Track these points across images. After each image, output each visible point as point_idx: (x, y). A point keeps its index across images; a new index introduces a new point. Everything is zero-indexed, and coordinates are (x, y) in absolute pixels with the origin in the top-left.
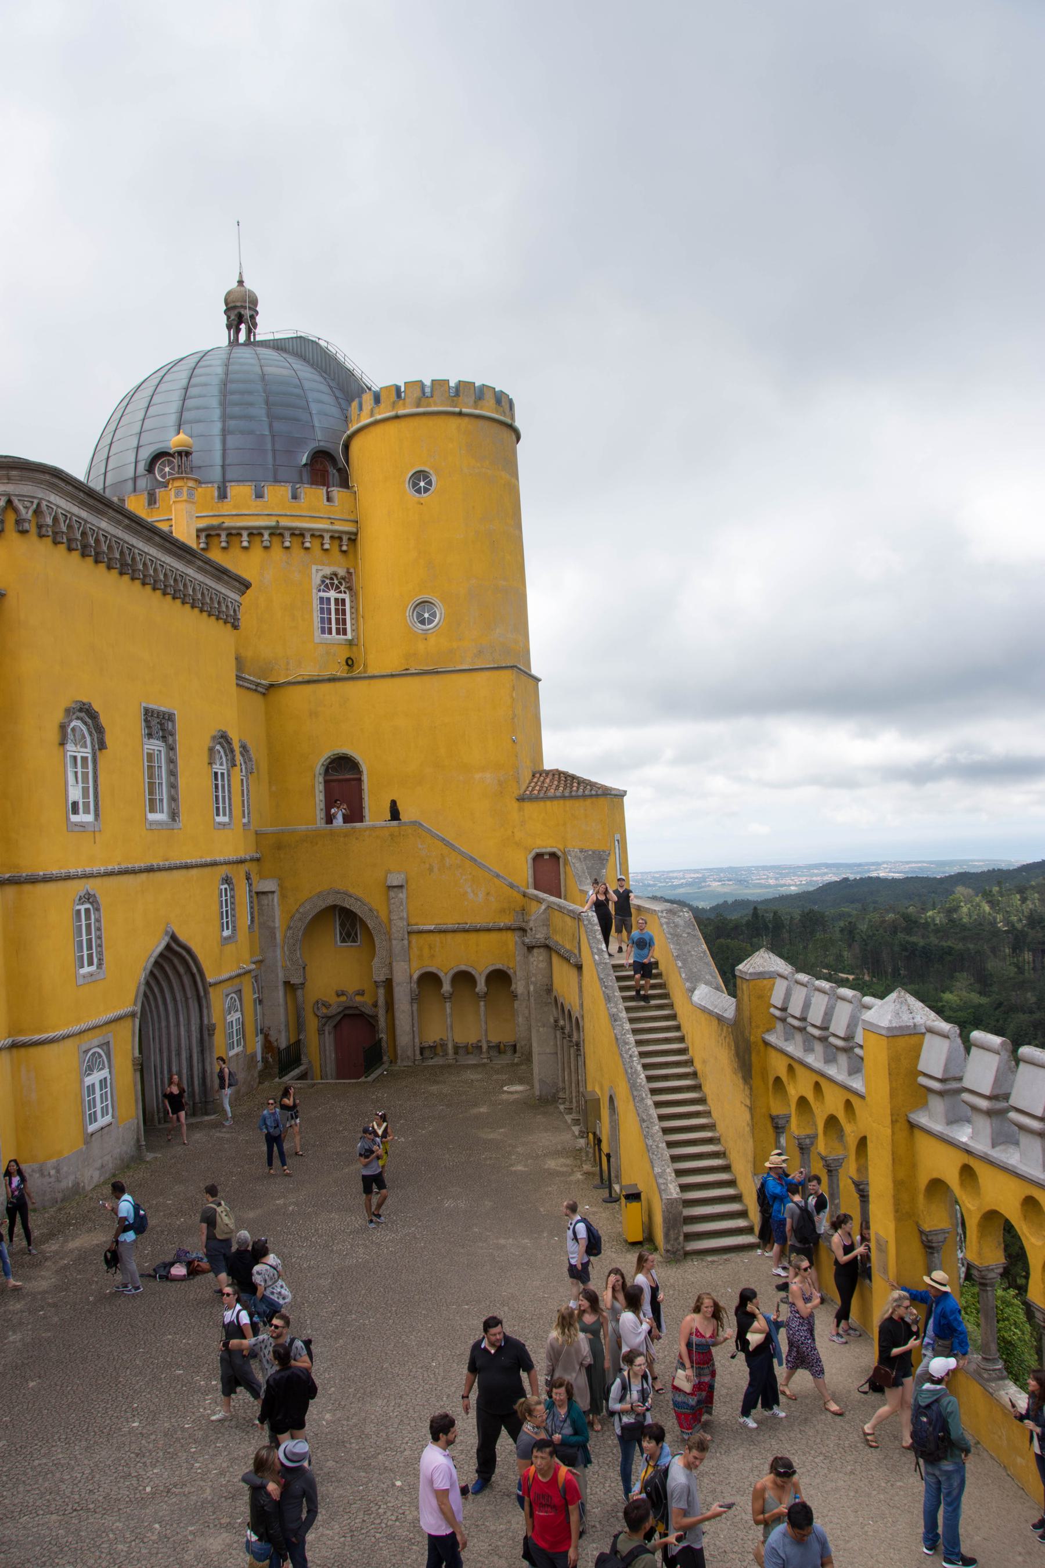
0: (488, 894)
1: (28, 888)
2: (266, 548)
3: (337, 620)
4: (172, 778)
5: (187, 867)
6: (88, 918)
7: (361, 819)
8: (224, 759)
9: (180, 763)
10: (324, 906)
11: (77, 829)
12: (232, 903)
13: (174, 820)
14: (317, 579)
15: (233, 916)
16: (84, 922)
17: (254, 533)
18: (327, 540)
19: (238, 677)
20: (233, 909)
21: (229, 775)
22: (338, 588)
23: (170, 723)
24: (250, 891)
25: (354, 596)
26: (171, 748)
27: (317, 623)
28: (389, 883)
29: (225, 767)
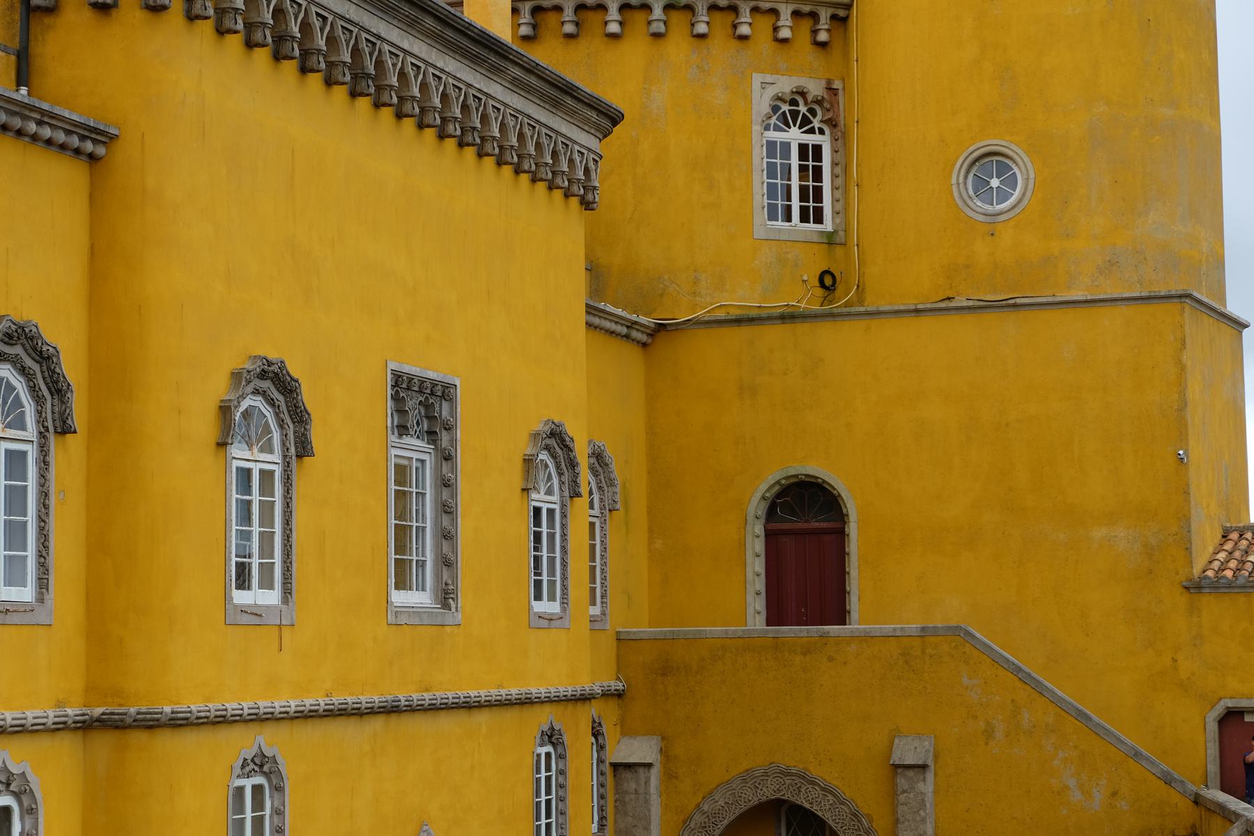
0: (1114, 794)
1: (138, 738)
2: (657, 36)
3: (804, 192)
4: (446, 521)
5: (469, 706)
6: (258, 804)
7: (841, 617)
8: (555, 481)
9: (463, 486)
10: (755, 801)
11: (246, 619)
12: (561, 786)
13: (446, 606)
14: (762, 104)
15: (562, 813)
16: (249, 814)
18: (786, 19)
19: (590, 310)
20: (561, 799)
21: (564, 516)
22: (806, 121)
23: (445, 405)
24: (600, 761)
26: (447, 457)
27: (760, 198)
28: (896, 759)
29: (555, 498)
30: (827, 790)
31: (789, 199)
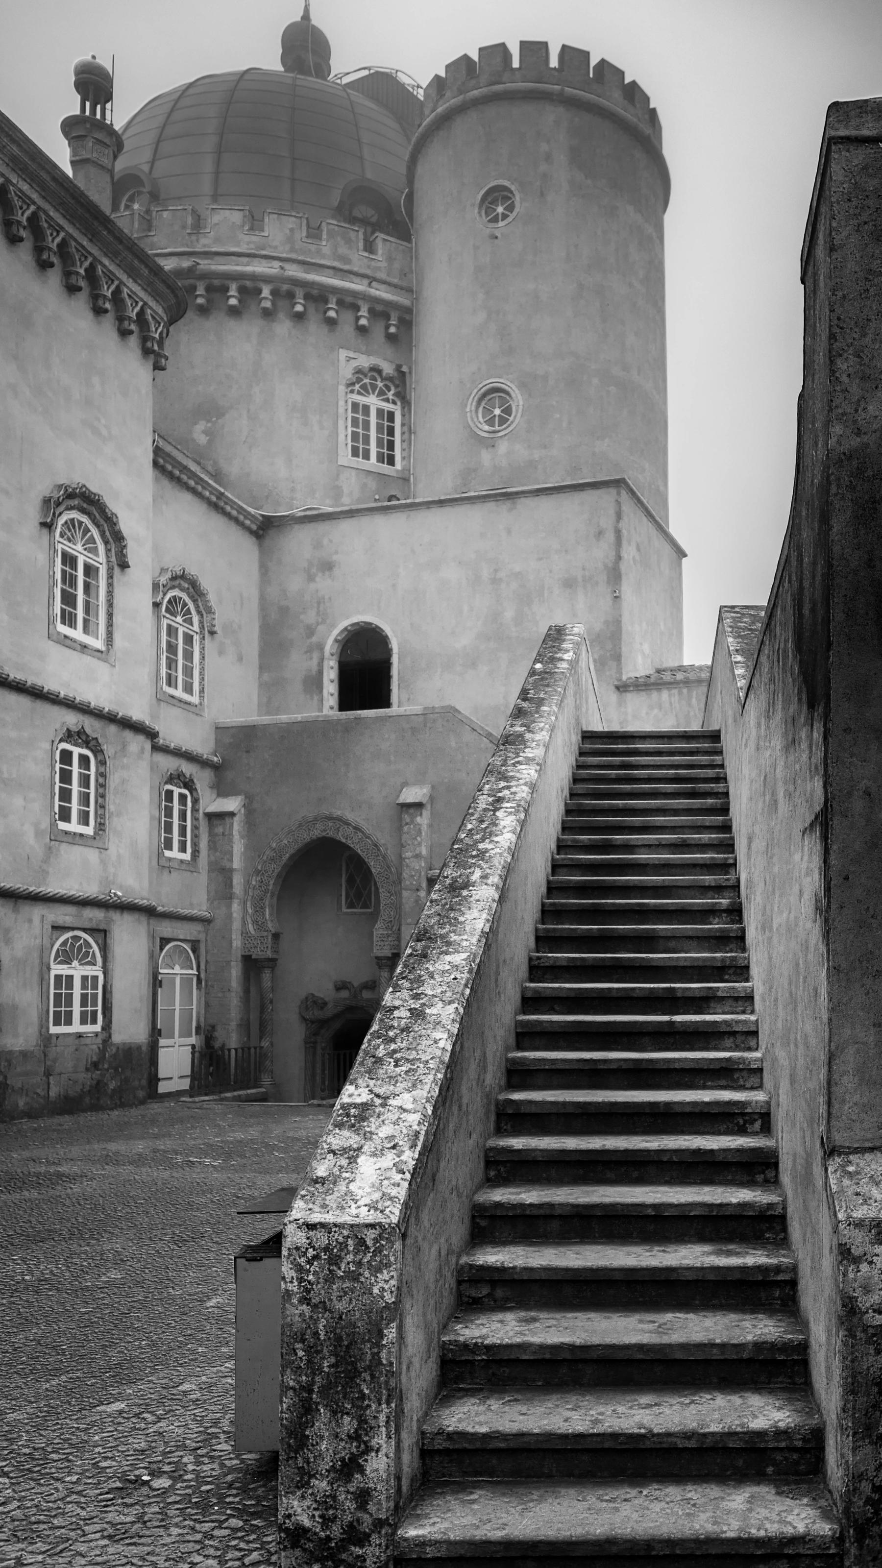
10: (308, 839)
14: (347, 372)
17: (249, 290)
18: (364, 312)
22: (381, 393)
25: (403, 398)
28: (401, 800)
30: (357, 829)
31: (368, 443)
